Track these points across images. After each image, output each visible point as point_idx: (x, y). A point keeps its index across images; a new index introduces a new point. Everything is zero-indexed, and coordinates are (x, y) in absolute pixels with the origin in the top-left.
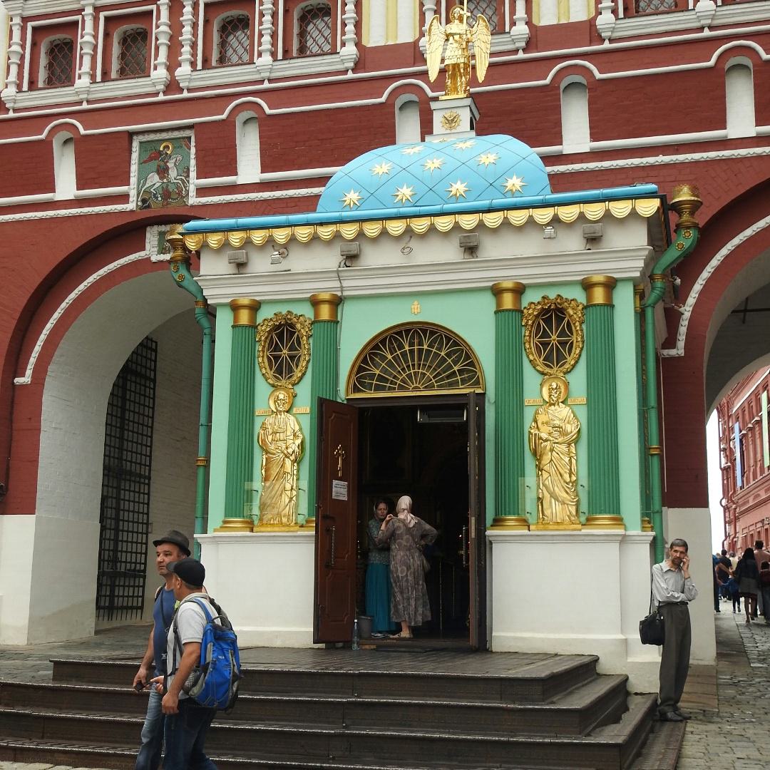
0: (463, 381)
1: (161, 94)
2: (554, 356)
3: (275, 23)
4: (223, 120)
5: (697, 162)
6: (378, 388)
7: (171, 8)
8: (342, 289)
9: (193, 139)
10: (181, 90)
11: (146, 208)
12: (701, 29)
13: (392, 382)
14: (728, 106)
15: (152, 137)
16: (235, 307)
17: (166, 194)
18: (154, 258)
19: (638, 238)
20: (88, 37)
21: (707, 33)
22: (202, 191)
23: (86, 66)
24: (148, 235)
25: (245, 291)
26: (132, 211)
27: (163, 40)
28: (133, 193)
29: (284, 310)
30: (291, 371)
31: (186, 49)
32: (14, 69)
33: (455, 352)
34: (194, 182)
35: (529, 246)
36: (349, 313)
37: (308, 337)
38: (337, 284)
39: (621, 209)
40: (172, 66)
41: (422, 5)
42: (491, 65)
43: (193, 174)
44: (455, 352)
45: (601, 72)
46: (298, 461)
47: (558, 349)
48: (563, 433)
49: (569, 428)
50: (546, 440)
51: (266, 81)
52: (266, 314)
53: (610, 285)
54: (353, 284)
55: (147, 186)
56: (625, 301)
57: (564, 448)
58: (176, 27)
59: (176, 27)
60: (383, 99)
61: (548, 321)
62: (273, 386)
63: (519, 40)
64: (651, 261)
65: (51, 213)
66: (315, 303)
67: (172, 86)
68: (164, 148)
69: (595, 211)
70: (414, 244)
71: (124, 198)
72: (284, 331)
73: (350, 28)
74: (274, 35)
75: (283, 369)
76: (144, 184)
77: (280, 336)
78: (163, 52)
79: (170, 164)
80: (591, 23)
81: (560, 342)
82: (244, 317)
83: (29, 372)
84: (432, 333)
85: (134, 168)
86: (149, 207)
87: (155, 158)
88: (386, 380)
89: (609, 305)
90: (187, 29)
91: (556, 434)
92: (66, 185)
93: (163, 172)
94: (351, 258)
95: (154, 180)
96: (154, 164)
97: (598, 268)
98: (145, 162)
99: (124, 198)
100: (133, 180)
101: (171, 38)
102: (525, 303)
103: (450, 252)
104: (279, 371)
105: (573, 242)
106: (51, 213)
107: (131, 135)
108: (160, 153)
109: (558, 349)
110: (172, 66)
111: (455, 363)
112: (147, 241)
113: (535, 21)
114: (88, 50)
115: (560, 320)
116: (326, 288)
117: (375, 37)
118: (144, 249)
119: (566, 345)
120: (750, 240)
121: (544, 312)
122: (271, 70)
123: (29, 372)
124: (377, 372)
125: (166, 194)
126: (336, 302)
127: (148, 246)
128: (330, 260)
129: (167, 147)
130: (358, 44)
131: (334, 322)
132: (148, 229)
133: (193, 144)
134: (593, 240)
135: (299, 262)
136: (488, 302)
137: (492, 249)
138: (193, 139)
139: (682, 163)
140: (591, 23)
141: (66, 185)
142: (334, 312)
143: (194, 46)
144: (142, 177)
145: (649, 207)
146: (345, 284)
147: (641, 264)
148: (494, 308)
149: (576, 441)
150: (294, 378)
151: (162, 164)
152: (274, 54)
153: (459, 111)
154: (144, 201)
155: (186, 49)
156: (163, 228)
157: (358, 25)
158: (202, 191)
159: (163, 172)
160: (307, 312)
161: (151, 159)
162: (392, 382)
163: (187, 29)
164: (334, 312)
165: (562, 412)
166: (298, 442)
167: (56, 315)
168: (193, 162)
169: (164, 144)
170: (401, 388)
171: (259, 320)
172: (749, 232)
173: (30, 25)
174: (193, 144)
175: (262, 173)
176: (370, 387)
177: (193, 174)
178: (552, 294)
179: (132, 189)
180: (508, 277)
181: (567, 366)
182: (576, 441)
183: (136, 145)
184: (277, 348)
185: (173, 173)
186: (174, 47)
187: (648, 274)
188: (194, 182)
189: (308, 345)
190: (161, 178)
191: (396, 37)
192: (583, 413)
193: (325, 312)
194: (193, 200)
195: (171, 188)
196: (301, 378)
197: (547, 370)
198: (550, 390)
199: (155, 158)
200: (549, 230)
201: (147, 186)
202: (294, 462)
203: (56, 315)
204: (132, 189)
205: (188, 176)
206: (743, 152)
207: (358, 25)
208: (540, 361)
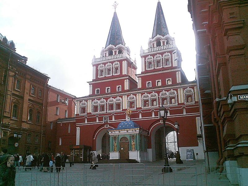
22: (109, 122)
34: (109, 121)
35: (131, 131)
53: (137, 134)
58: (107, 108)
67: (106, 112)
87: (105, 119)
92: (97, 121)
93: (106, 120)
97: (136, 133)
99: (103, 122)
105: (134, 131)
116: (118, 134)
126: (118, 135)
137: (129, 131)
141: (97, 121)
144: (104, 121)
145: (139, 129)
158: (109, 122)
159: (106, 120)
180: (130, 134)
186: (107, 109)
199: (105, 119)
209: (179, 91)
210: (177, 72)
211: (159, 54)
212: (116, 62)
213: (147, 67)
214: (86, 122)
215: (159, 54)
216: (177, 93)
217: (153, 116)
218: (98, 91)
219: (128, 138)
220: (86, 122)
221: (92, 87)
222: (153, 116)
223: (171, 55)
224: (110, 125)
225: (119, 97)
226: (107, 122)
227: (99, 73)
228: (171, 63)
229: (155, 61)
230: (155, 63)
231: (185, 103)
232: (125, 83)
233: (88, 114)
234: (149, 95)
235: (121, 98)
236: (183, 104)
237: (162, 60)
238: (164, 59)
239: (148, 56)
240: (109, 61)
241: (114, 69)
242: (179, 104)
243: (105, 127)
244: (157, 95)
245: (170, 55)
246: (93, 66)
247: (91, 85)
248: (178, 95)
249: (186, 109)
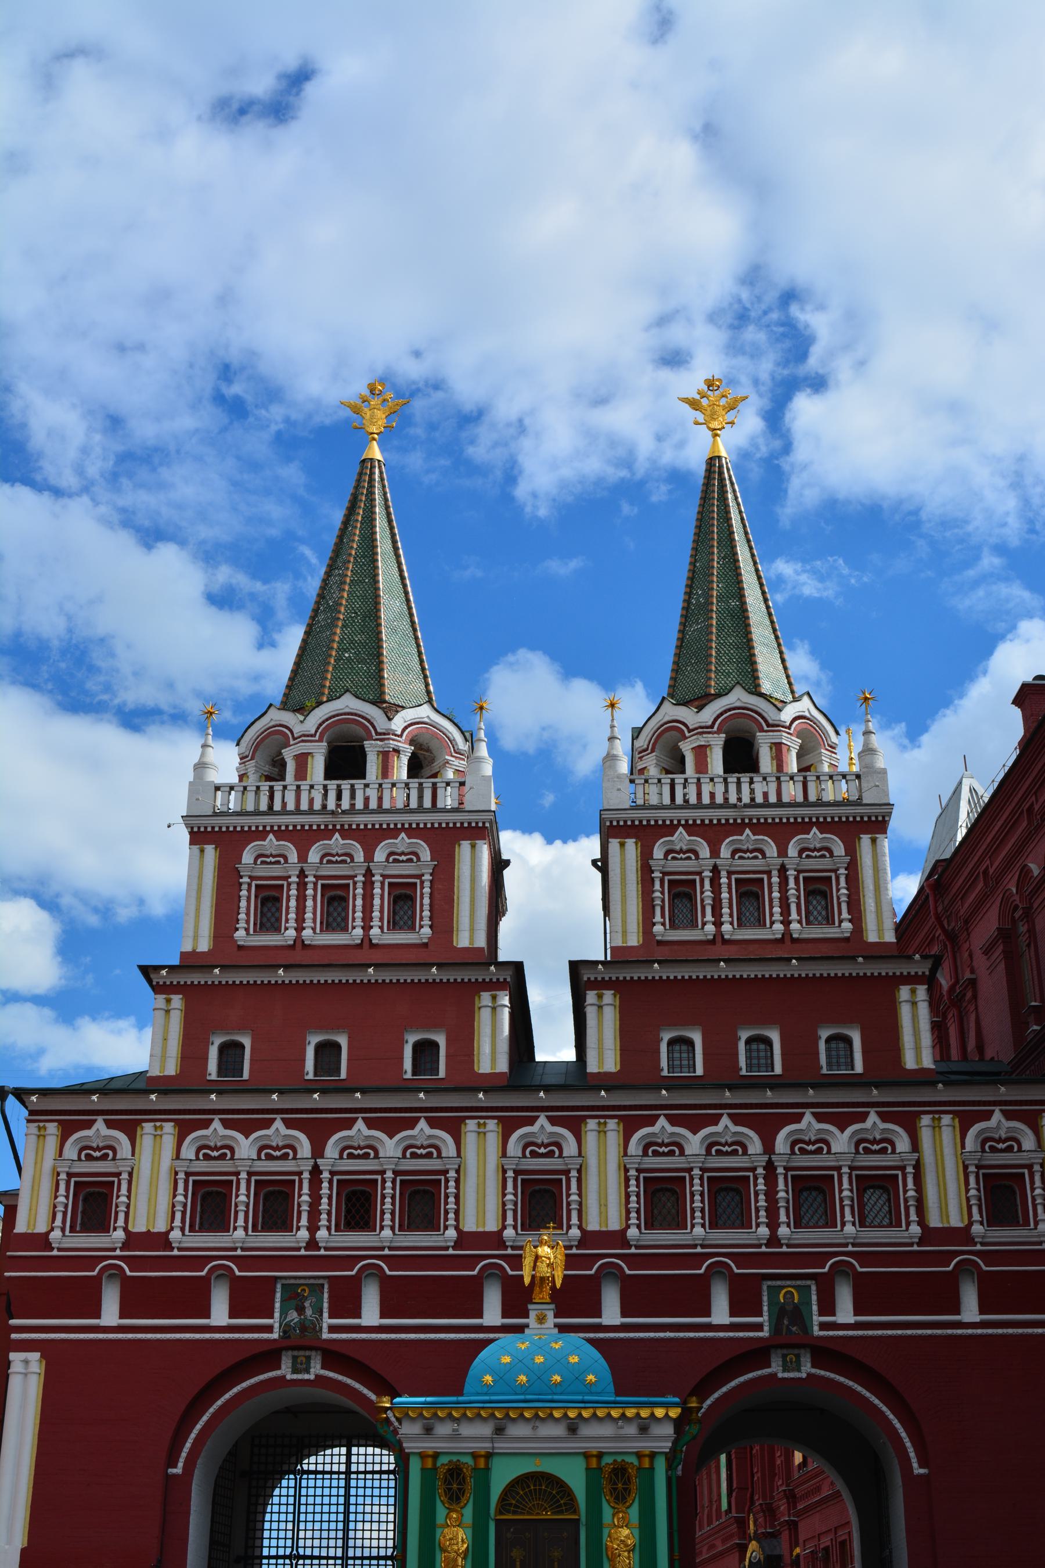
0: (567, 1510)
1: (303, 1250)
2: (620, 1498)
3: (393, 1204)
4: (352, 1276)
5: (692, 1339)
6: (515, 1513)
7: (311, 1181)
8: (493, 1448)
9: (326, 1286)
10: (319, 1249)
11: (286, 1338)
12: (695, 1246)
13: (522, 1509)
14: (712, 1299)
15: (292, 1281)
16: (423, 1456)
17: (303, 1327)
18: (289, 1377)
19: (669, 1430)
20: (243, 1197)
21: (699, 1250)
23: (241, 1222)
24: (284, 1358)
25: (429, 1446)
26: (275, 1340)
27: (305, 1207)
28: (277, 1325)
29: (455, 1458)
30: (458, 1499)
31: (324, 1216)
32: (178, 1216)
33: (561, 1491)
34: (327, 1321)
35: (607, 1430)
36: (496, 1464)
37: (471, 1477)
38: (490, 1445)
39: (660, 1412)
40: (313, 1228)
41: (504, 1204)
42: (565, 1277)
43: (326, 1315)
44: (561, 1491)
45: (629, 1270)
46: (464, 1558)
47: (622, 1494)
48: (626, 1545)
49: (629, 1542)
50: (617, 1549)
51: (386, 1249)
52: (443, 1460)
53: (653, 1456)
54: (501, 1446)
55: (287, 1320)
56: (660, 1465)
57: (626, 1554)
58: (315, 1198)
59: (315, 1198)
60: (475, 1273)
61: (616, 1475)
62: (448, 1508)
63: (574, 1240)
64: (675, 1442)
65: (207, 1336)
66: (475, 1456)
67: (312, 1244)
68: (302, 1290)
69: (645, 1413)
70: (538, 1424)
71: (269, 1329)
72: (455, 1472)
73: (451, 1215)
74: (393, 1213)
75: (455, 1498)
76: (285, 1318)
77: (452, 1475)
78: (305, 1217)
79: (307, 1304)
80: (623, 1232)
81: (623, 1488)
82: (429, 1463)
83: (180, 1465)
84: (547, 1479)
85: (277, 1305)
86: (289, 1337)
87: (294, 1297)
88: (518, 1507)
89: (652, 1468)
90: (325, 1200)
91: (622, 1546)
92: (220, 1314)
93: (301, 1310)
94: (499, 1430)
95: (293, 1316)
96: (294, 1302)
97: (646, 1445)
98: (286, 1300)
99: (269, 1329)
100: (277, 1315)
101: (311, 1205)
102: (603, 1463)
103: (559, 1430)
104: (451, 1499)
105: (632, 1430)
106: (207, 1336)
107: (276, 1278)
108: (298, 1294)
109: (622, 1494)
110: (313, 1228)
111: (562, 1498)
112: (283, 1362)
113: (584, 1226)
114: (242, 1208)
115: (623, 1475)
117: (470, 1225)
118: (279, 1368)
119: (627, 1491)
120: (725, 1394)
121: (614, 1469)
122: (391, 1242)
123: (180, 1465)
124: (514, 1502)
125: (303, 1327)
126: (489, 1456)
127: (283, 1367)
128: (485, 1430)
129: (304, 1290)
130: (457, 1228)
131: (488, 1469)
132: (284, 1353)
133: (326, 1290)
134: (644, 1429)
135: (467, 1430)
136: (580, 1464)
138: (326, 1286)
139: (682, 1339)
140: (623, 1232)
141: (220, 1314)
142: (487, 1463)
143: (329, 1213)
144: (284, 1313)
145: (674, 1413)
146: (496, 1445)
147: (670, 1444)
148: (584, 1466)
149: (633, 1550)
150: (462, 1504)
151: (300, 1303)
152: (392, 1228)
153: (547, 1312)
154: (285, 1332)
155: (324, 1216)
156: (296, 1353)
157: (457, 1213)
158: (332, 1329)
159: (301, 1310)
160: (469, 1460)
161: (290, 1298)
162: (522, 1509)
163: (325, 1200)
164: (487, 1463)
165: (625, 1532)
166: (465, 1546)
167: (205, 1418)
168: (326, 1305)
169: (302, 1288)
170: (529, 1514)
171: (438, 1464)
172: (724, 1389)
173: (191, 1179)
174: (326, 1290)
175: (381, 1318)
176: (509, 1512)
177: (326, 1315)
178: (619, 1459)
179: (275, 1322)
180: (594, 1447)
181: (628, 1504)
182: (633, 1550)
183: (279, 1287)
184: (450, 1483)
185: (309, 1312)
187: (674, 1449)
188: (327, 1321)
189: (471, 1482)
190: (299, 1315)
191: (484, 1225)
192: (636, 1532)
193: (482, 1463)
194: (326, 1336)
195: (307, 1324)
196: (466, 1504)
197: (616, 1506)
198: (618, 1519)
200: (620, 1423)
201: (287, 1320)
202: (462, 1559)
203: (205, 1418)
204: (275, 1322)
205: (321, 1315)
206: (721, 1334)
207: (457, 1213)
208: (612, 1500)
209: (926, 1136)
210: (904, 992)
211: (759, 827)
212: (402, 842)
213: (658, 918)
214: (110, 1314)
215: (759, 827)
216: (915, 1146)
217: (720, 1313)
218: (231, 1052)
219: (577, 1483)
220: (110, 1314)
221: (176, 1019)
222: (720, 1313)
223: (852, 851)
224: (333, 1356)
225: (433, 1123)
226: (310, 1328)
227: (243, 904)
228: (845, 915)
229: (724, 880)
230: (725, 895)
231: (977, 1229)
232: (484, 1017)
233: (132, 1240)
234: (694, 1143)
235: (446, 1138)
236: (963, 1235)
237: (775, 880)
238: (791, 873)
239: (669, 829)
240: (346, 819)
241: (377, 891)
242: (929, 1235)
243: (285, 1370)
244: (755, 1146)
245: (839, 849)
246: (198, 837)
247: (177, 1001)
248: (918, 1166)
249: (982, 1276)
